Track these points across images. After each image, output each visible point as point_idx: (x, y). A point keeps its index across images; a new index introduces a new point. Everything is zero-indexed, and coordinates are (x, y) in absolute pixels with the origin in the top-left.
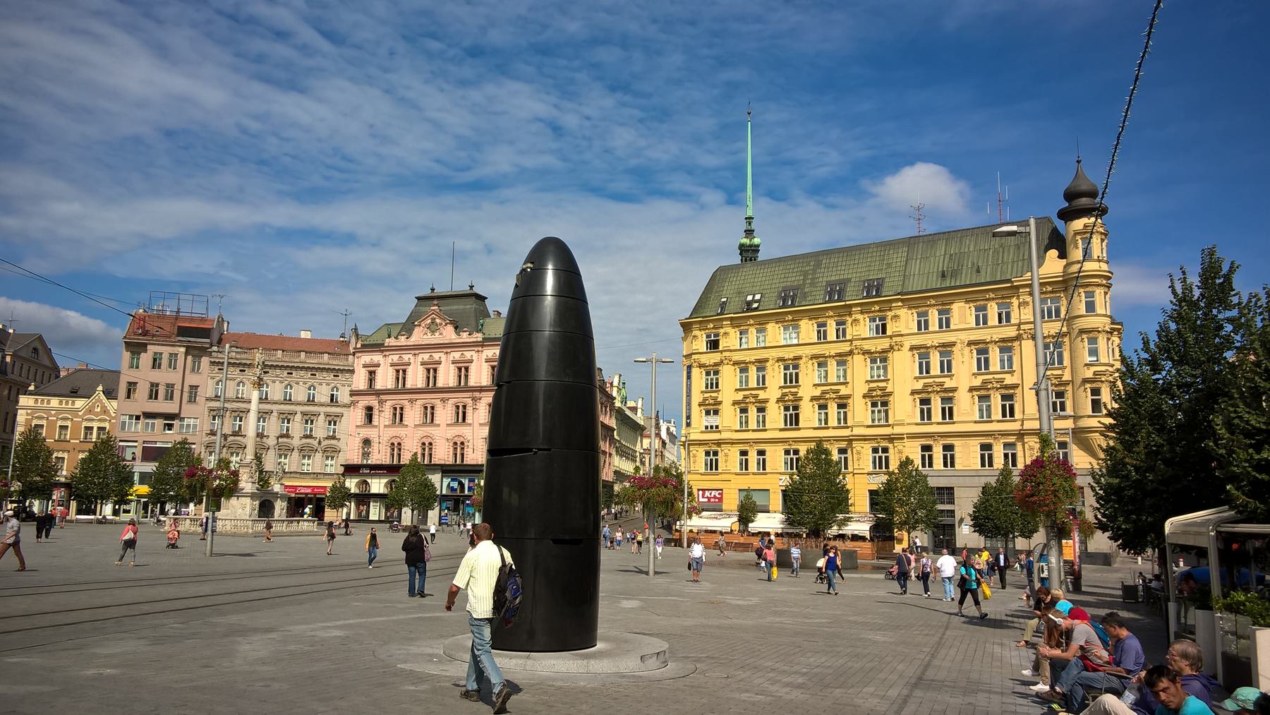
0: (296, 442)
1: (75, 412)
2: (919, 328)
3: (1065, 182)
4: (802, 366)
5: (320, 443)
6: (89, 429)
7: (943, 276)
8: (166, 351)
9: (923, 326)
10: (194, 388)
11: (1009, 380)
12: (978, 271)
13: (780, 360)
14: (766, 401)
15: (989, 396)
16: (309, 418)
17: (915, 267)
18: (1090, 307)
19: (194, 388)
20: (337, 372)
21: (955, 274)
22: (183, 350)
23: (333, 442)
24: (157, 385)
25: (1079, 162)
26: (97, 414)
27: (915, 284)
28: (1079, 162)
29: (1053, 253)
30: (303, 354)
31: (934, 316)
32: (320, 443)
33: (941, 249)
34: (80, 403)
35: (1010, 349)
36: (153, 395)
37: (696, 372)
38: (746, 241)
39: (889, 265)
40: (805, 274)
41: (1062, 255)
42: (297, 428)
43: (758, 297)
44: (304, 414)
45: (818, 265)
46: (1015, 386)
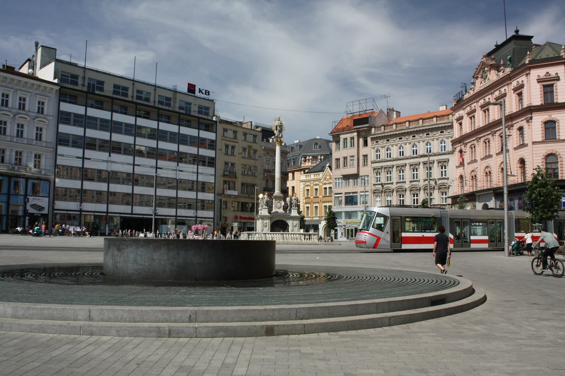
0: (422, 184)
1: (319, 180)
5: (436, 183)
6: (326, 188)
8: (348, 136)
10: (365, 156)
16: (429, 166)
19: (365, 156)
20: (442, 129)
22: (356, 134)
23: (445, 181)
24: (339, 159)
26: (328, 180)
30: (435, 119)
32: (436, 183)
34: (321, 174)
36: (345, 165)
42: (422, 172)
44: (425, 163)
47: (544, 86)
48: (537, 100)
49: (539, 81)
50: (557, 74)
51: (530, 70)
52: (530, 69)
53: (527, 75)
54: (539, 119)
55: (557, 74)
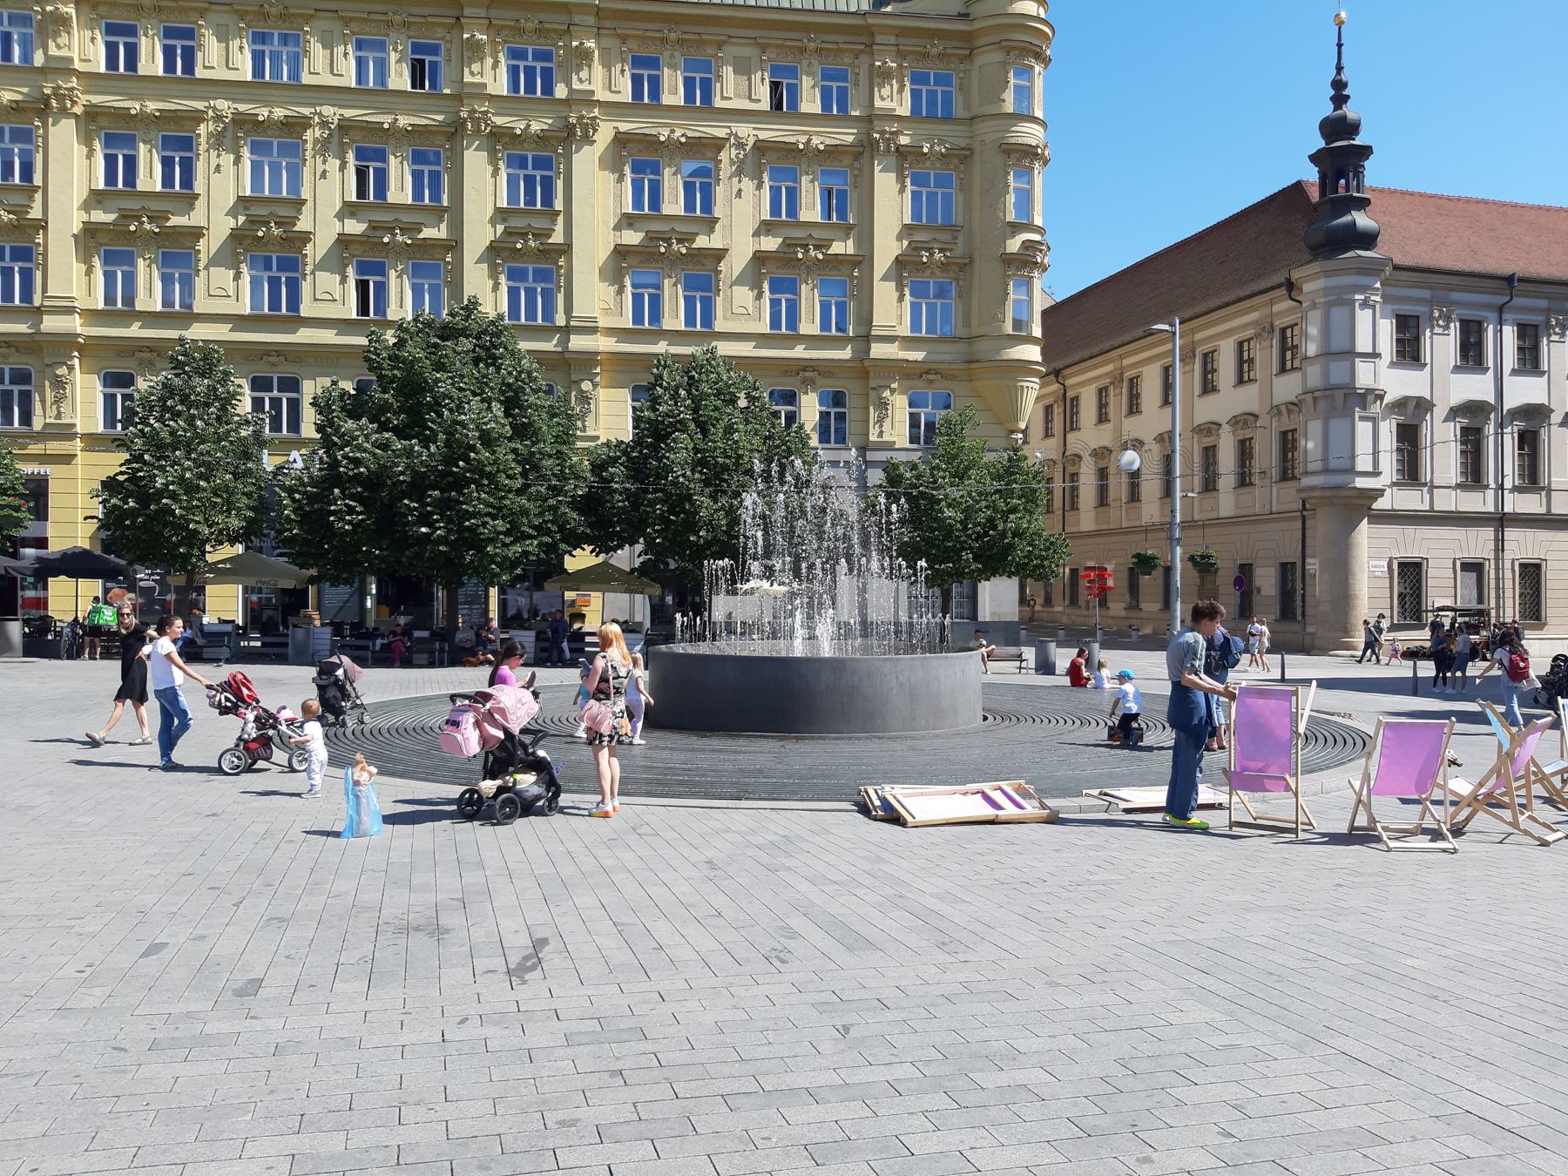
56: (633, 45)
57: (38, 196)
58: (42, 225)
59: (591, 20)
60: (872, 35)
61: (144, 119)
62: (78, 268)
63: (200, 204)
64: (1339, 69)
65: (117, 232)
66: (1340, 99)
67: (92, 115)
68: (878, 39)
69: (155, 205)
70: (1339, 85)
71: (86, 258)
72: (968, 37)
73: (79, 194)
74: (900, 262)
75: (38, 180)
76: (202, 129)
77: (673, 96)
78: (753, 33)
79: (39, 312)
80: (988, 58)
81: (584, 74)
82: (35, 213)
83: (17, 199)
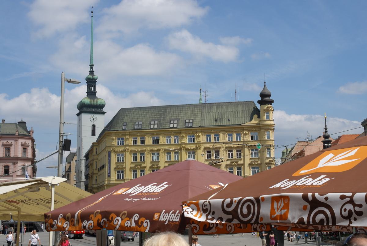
2: (207, 140)
3: (260, 90)
4: (160, 154)
7: (216, 121)
9: (209, 140)
11: (240, 162)
12: (229, 120)
13: (151, 151)
14: (145, 167)
15: (233, 168)
17: (205, 116)
18: (269, 137)
21: (220, 120)
25: (265, 83)
27: (206, 123)
28: (265, 83)
29: (256, 116)
31: (213, 137)
33: (214, 110)
35: (240, 151)
37: (113, 155)
38: (91, 77)
39: (195, 114)
40: (160, 115)
41: (259, 117)
43: (140, 123)
45: (166, 111)
46: (242, 165)
47: (23, 148)
48: (20, 154)
49: (22, 145)
50: (28, 144)
51: (18, 139)
52: (19, 138)
53: (16, 140)
54: (20, 164)
55: (28, 144)
56: (206, 133)
57: (124, 164)
58: (125, 168)
59: (200, 131)
60: (244, 128)
61: (138, 151)
62: (129, 172)
63: (146, 163)
64: (326, 126)
65: (135, 167)
66: (326, 132)
67: (131, 151)
68: (245, 129)
69: (140, 164)
70: (326, 129)
71: (131, 171)
72: (260, 127)
73: (129, 163)
74: (249, 164)
75: (124, 161)
76: (146, 152)
77: (213, 140)
78: (224, 130)
79: (124, 180)
80: (262, 130)
81: (199, 139)
82: (124, 166)
83: (122, 164)
